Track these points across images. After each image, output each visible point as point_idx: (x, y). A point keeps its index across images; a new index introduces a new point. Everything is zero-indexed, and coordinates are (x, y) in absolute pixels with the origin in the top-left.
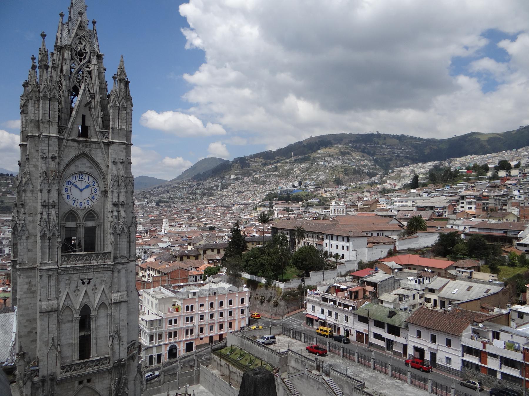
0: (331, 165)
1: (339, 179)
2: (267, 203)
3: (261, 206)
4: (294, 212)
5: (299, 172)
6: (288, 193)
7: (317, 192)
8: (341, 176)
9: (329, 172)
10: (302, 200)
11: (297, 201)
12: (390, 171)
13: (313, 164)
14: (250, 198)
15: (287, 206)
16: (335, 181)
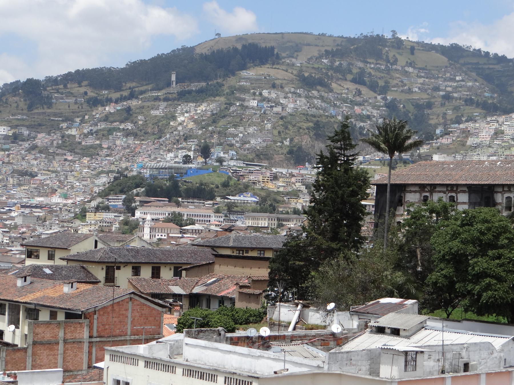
0: (278, 109)
1: (300, 148)
2: (117, 201)
3: (97, 209)
4: (197, 227)
5: (191, 125)
6: (172, 178)
7: (252, 177)
8: (305, 141)
9: (274, 128)
10: (212, 198)
11: (199, 198)
12: (438, 131)
13: (231, 104)
14: (54, 192)
15: (177, 210)
16: (290, 152)
